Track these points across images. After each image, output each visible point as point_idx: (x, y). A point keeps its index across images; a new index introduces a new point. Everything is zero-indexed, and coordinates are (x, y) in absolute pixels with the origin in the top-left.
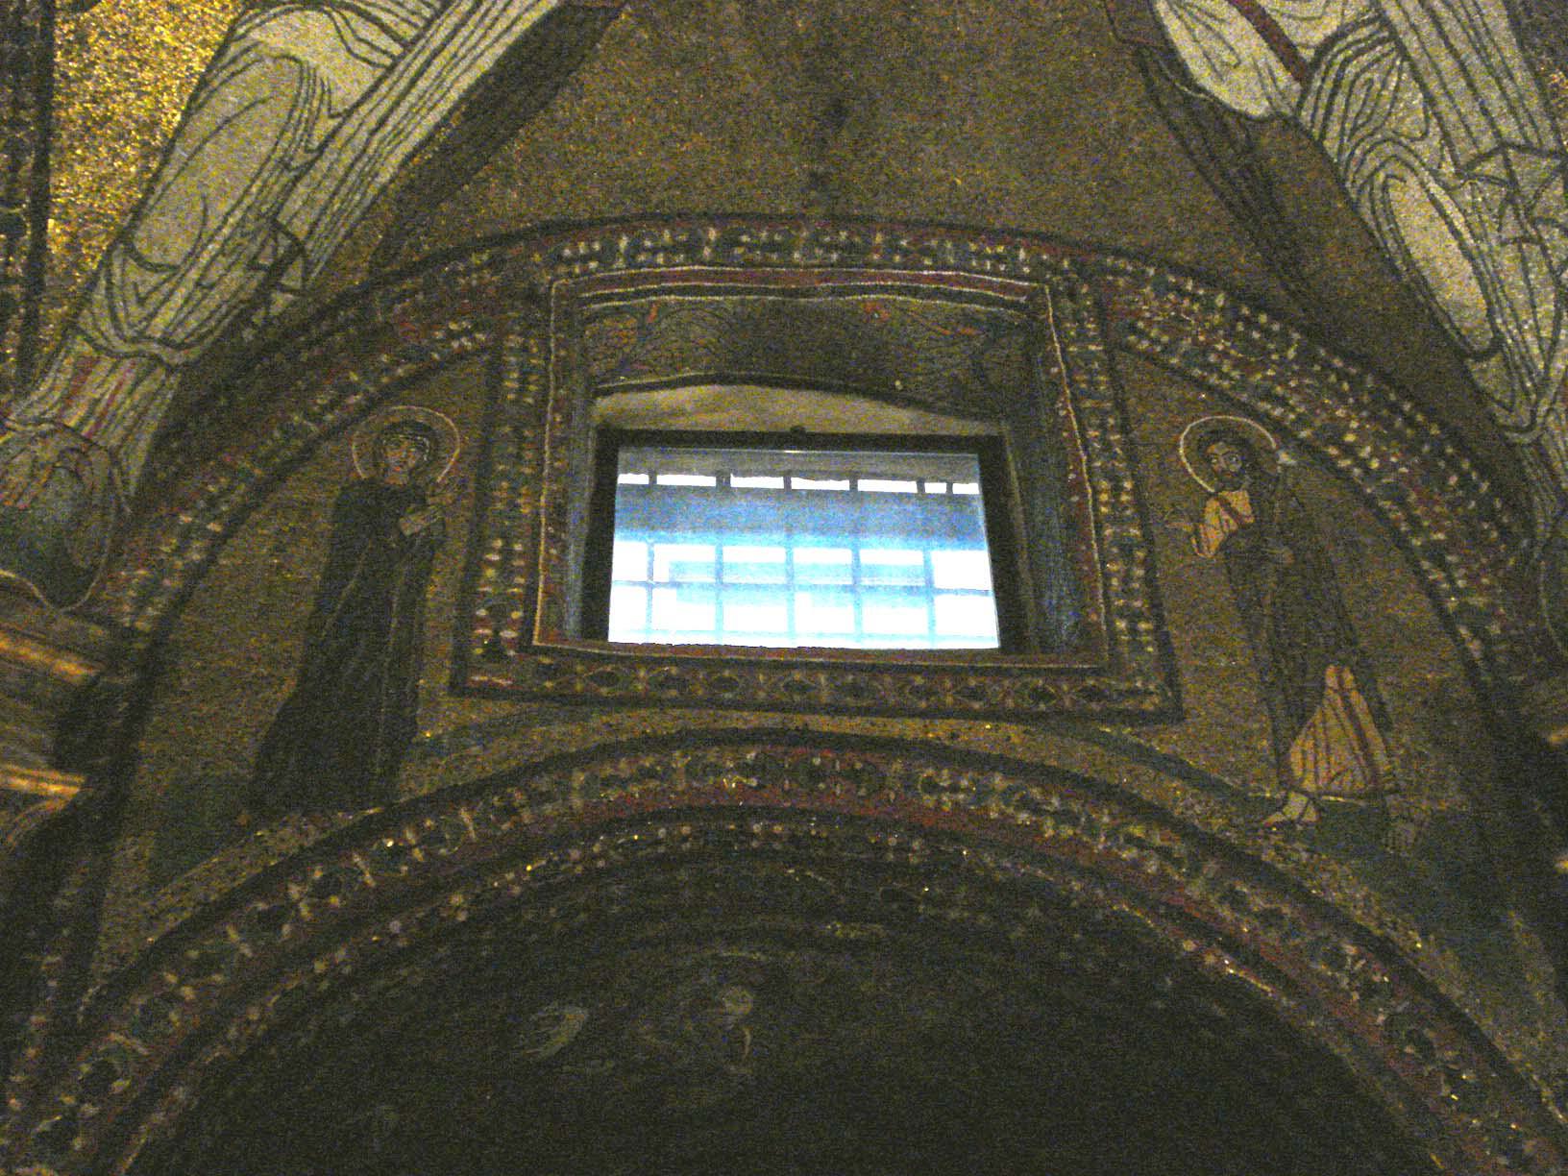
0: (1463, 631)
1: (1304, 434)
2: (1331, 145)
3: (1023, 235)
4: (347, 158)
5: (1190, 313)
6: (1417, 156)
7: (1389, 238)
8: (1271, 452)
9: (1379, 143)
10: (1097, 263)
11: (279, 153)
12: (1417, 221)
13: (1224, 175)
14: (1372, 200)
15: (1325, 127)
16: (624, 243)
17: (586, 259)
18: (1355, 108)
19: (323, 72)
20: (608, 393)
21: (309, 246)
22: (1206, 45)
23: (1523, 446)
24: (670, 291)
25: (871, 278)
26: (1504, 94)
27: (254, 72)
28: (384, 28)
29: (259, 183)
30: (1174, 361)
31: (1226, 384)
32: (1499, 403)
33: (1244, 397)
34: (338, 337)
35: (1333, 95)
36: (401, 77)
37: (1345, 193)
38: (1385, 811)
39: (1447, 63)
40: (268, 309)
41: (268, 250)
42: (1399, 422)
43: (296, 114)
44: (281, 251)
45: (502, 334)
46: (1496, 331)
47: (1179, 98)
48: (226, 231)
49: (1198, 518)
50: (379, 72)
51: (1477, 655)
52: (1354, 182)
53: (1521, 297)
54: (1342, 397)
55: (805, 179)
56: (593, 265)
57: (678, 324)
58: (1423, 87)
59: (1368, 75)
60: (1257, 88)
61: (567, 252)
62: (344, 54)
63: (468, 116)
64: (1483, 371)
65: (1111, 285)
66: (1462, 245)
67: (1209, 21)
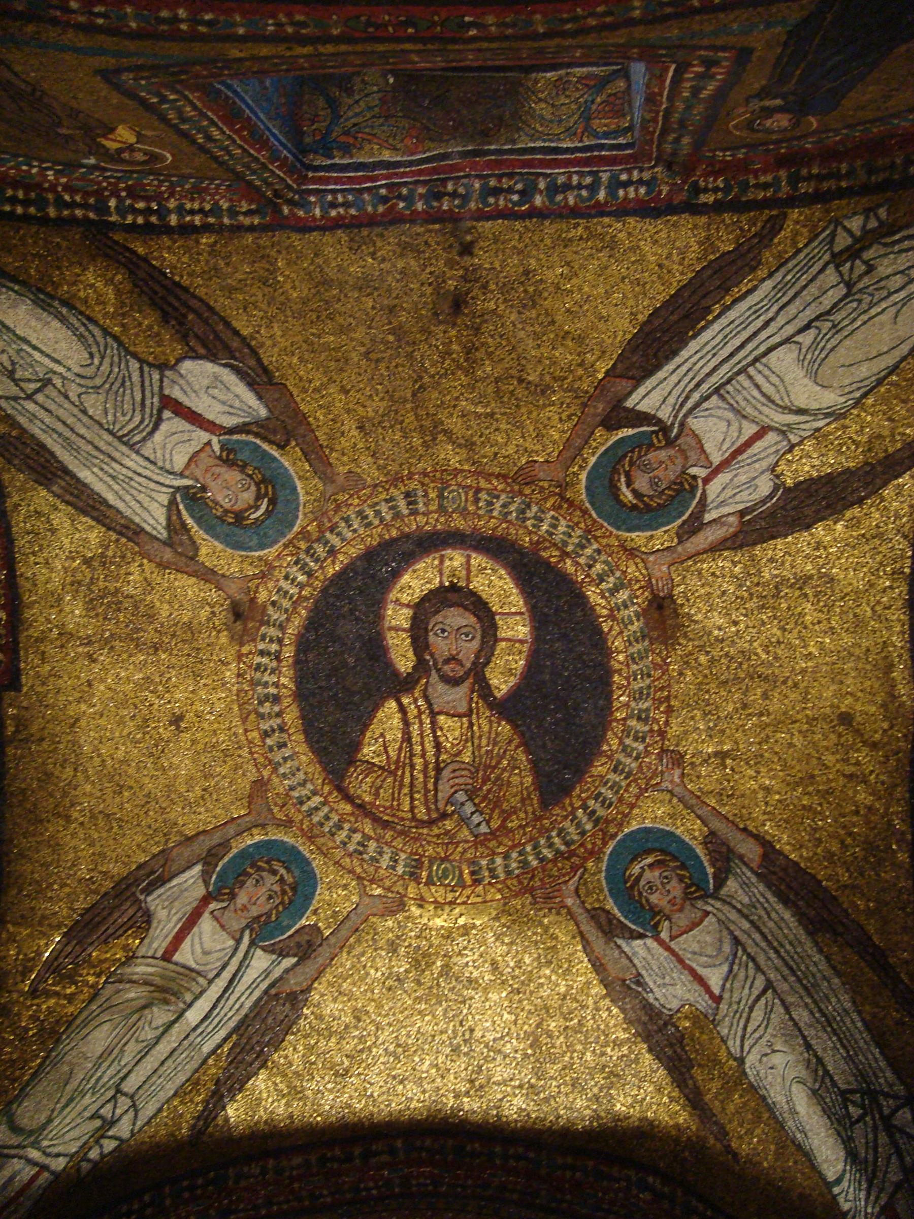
2: (134, 365)
4: (792, 310)
5: (192, 200)
6: (79, 385)
7: (77, 324)
9: (105, 382)
10: (264, 217)
11: (838, 337)
12: (63, 345)
14: (97, 344)
15: (142, 376)
16: (602, 195)
18: (127, 398)
21: (827, 257)
22: (231, 396)
24: (567, 150)
25: (420, 173)
26: (42, 422)
27: (847, 382)
28: (757, 386)
34: (815, 171)
36: (751, 352)
37: (116, 338)
39: (83, 431)
40: (864, 226)
43: (822, 356)
44: (848, 265)
47: (237, 354)
48: (884, 305)
50: (764, 360)
52: (112, 348)
55: (476, 251)
56: (624, 177)
57: (560, 121)
58: (91, 417)
59: (127, 418)
61: (642, 190)
62: (786, 379)
63: (708, 310)
65: (251, 202)
67: (232, 410)
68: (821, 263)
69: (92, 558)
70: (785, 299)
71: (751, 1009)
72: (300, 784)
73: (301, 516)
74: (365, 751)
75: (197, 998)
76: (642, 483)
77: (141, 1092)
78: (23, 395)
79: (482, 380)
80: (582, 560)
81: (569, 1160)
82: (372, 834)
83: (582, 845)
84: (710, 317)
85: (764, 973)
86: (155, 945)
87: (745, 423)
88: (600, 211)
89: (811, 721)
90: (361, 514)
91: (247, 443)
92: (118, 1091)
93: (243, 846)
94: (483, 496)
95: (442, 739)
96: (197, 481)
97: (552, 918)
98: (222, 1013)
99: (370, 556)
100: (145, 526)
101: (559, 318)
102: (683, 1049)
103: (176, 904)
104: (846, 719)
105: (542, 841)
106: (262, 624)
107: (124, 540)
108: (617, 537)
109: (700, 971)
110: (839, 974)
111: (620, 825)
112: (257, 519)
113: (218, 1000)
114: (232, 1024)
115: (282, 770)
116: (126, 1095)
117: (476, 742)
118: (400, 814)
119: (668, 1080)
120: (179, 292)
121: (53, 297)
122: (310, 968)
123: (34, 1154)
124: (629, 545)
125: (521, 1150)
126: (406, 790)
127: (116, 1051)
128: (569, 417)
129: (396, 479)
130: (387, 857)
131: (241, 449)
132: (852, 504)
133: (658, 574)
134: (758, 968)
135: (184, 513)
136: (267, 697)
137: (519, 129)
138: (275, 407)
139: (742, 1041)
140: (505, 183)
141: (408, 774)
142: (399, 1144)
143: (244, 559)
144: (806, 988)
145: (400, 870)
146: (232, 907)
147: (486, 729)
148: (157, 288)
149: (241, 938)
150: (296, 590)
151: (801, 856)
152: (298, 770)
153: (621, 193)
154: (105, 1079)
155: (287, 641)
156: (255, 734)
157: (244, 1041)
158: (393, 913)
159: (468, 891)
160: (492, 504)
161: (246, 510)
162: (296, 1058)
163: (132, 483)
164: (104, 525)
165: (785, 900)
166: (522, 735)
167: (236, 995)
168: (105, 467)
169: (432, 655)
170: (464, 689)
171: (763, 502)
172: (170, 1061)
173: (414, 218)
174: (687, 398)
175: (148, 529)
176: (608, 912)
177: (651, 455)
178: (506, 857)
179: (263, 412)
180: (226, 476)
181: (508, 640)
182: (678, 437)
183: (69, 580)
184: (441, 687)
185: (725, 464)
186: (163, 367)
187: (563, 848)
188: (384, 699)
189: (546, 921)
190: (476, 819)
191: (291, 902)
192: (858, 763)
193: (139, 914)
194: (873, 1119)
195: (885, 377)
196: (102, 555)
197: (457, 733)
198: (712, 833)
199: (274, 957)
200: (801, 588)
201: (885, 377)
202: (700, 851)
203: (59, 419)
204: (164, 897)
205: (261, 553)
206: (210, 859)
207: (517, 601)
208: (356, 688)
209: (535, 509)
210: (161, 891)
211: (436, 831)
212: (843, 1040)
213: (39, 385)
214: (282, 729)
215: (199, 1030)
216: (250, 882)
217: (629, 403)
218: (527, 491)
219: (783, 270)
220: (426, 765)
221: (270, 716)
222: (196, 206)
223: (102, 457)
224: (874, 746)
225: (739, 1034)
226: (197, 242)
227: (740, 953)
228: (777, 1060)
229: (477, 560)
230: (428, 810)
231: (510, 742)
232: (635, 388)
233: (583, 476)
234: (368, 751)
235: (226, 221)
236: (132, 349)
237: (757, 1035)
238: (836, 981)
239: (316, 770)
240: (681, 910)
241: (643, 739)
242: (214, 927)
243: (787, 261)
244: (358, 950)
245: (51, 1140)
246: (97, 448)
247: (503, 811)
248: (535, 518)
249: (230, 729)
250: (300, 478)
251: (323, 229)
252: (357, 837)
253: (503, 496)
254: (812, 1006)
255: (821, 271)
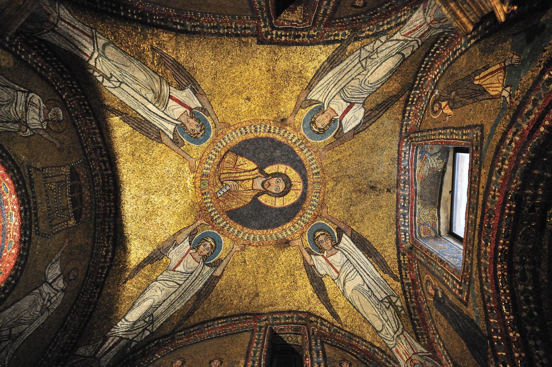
0: (469, 45)
1: (433, 88)
2: (366, 96)
3: (399, 149)
4: (373, 283)
5: (413, 114)
7: (382, 80)
8: (435, 96)
12: (377, 76)
13: (378, 113)
15: (362, 98)
16: (402, 228)
17: (406, 236)
18: (356, 93)
19: (356, 285)
20: (440, 232)
21: (389, 294)
23: (421, 41)
26: (350, 64)
27: (354, 298)
29: (371, 303)
30: (421, 117)
31: (425, 106)
32: (413, 48)
33: (427, 102)
35: (354, 98)
37: (375, 91)
38: (509, 65)
39: (346, 77)
40: (399, 306)
41: (386, 304)
42: (428, 66)
44: (387, 301)
45: (415, 257)
46: (396, 54)
49: (446, 115)
50: (358, 274)
51: (474, 41)
53: (388, 50)
54: (426, 79)
55: (388, 193)
56: (407, 234)
58: (351, 81)
59: (349, 93)
60: (358, 111)
61: (403, 239)
63: (370, 257)
64: (407, 54)
65: (410, 130)
66: (379, 66)
68: (387, 292)
69: (301, 73)
70: (375, 281)
71: (173, 281)
72: (229, 138)
73: (313, 141)
74: (240, 158)
75: (156, 107)
76: (322, 238)
77: (122, 90)
78: (361, 59)
79: (351, 194)
80: (299, 222)
81: (112, 227)
82: (215, 161)
83: (216, 224)
84: (369, 258)
85: (184, 283)
86: (174, 93)
87: (340, 268)
88: (398, 227)
89: (256, 285)
90: (313, 158)
91: (336, 127)
92: (122, 83)
93: (209, 121)
94: (318, 194)
95: (245, 182)
96: (326, 111)
97: (193, 217)
98: (152, 115)
99: (300, 161)
100: (312, 92)
101: (368, 216)
102: (156, 260)
103: (188, 99)
104: (257, 295)
105: (216, 212)
106: (279, 128)
107: (307, 85)
108: (306, 231)
109: (182, 263)
110: (185, 304)
111: (222, 234)
112: (312, 128)
113: (156, 114)
114: (148, 119)
115: (233, 133)
116: (120, 85)
117: (245, 192)
118: (222, 170)
119: (145, 257)
120: (385, 109)
121: (393, 73)
122: (170, 143)
123: (96, 55)
124: (304, 234)
125: (114, 211)
126: (229, 171)
127: (137, 82)
128: (340, 218)
129: (323, 170)
130: (208, 166)
131: (335, 125)
132: (318, 295)
133: (296, 242)
134: (185, 281)
135: (315, 106)
136: (256, 128)
137: (422, 205)
138: (347, 135)
139: (163, 280)
140: (407, 201)
141: (234, 172)
142: (109, 172)
143: (300, 123)
144: (181, 296)
145: (204, 171)
146: (189, 117)
147: (249, 194)
148: (388, 103)
149: (178, 121)
150: (290, 139)
151: (218, 287)
152: (234, 138)
153: (403, 233)
154: (126, 79)
155: (274, 135)
156: (245, 125)
157: (142, 122)
158: (190, 169)
159: (199, 192)
160: (316, 197)
161: (315, 125)
162: (137, 139)
163: (326, 90)
164: (312, 78)
165: (205, 285)
166: (247, 205)
167: (159, 120)
168: (333, 82)
169: (271, 179)
170: (261, 188)
171: (317, 272)
172: (134, 99)
173: (399, 175)
174: (346, 251)
175: (311, 93)
176: (196, 234)
177: (329, 241)
178: (211, 202)
179: (345, 132)
180: (326, 120)
181: (275, 201)
182: (335, 248)
183: (295, 65)
184: (261, 181)
185: (328, 262)
186: (364, 104)
187: (215, 218)
188: (257, 164)
189: (192, 216)
190: (222, 193)
191: (192, 137)
192: (245, 299)
193: (183, 86)
194: (146, 325)
195: (356, 309)
196: (303, 77)
197: (247, 186)
198: (222, 261)
199: (173, 132)
200: (293, 282)
201: (356, 309)
202: (216, 258)
203: (351, 70)
204: (190, 94)
205: (302, 129)
206: (203, 109)
207: (287, 203)
208: (260, 156)
209: (314, 208)
210: (192, 93)
211: (217, 181)
212: (166, 310)
213: (364, 66)
214: (246, 133)
215: (145, 108)
216: (197, 123)
217: (344, 235)
218: (319, 207)
219: (383, 280)
220: (237, 177)
221: (250, 129)
222: (411, 115)
223: (336, 81)
224: (250, 303)
225: (165, 279)
226: (400, 115)
227: (189, 275)
228: (159, 293)
229: (300, 193)
230: (224, 178)
231: (245, 201)
232: (348, 237)
233: (323, 222)
234: (240, 159)
235: (405, 123)
236: (371, 95)
237: (165, 284)
238: (183, 304)
239: (233, 143)
240: (199, 255)
241: (248, 239)
242: (181, 112)
243: (386, 282)
244: (177, 159)
245: (102, 61)
246: (339, 81)
247: (224, 200)
248: (311, 208)
249: (246, 116)
250: (325, 141)
251: (398, 151)
252: (214, 157)
253: (318, 200)
254: (176, 299)
255: (385, 293)
